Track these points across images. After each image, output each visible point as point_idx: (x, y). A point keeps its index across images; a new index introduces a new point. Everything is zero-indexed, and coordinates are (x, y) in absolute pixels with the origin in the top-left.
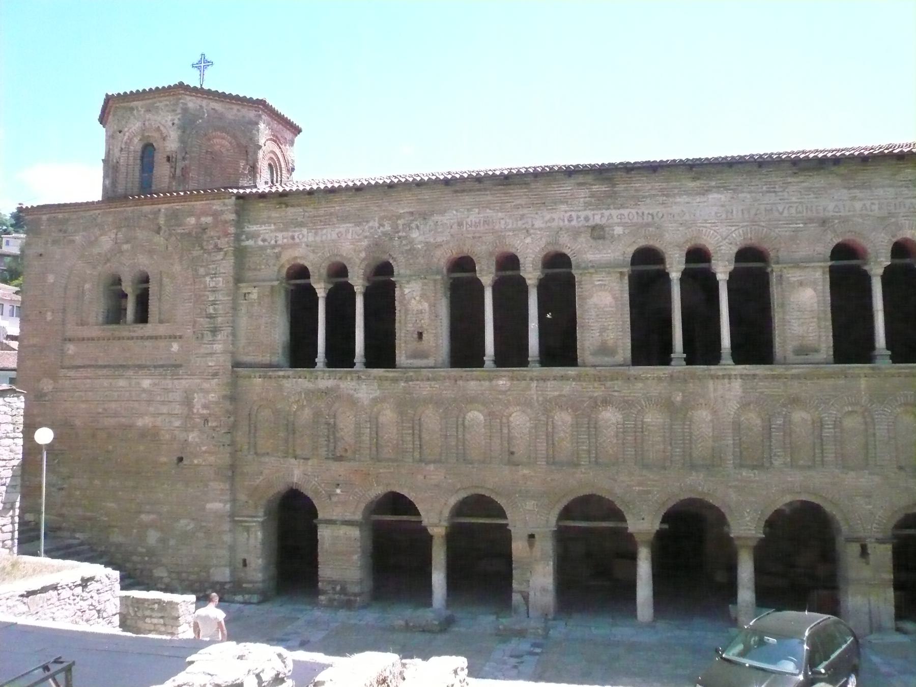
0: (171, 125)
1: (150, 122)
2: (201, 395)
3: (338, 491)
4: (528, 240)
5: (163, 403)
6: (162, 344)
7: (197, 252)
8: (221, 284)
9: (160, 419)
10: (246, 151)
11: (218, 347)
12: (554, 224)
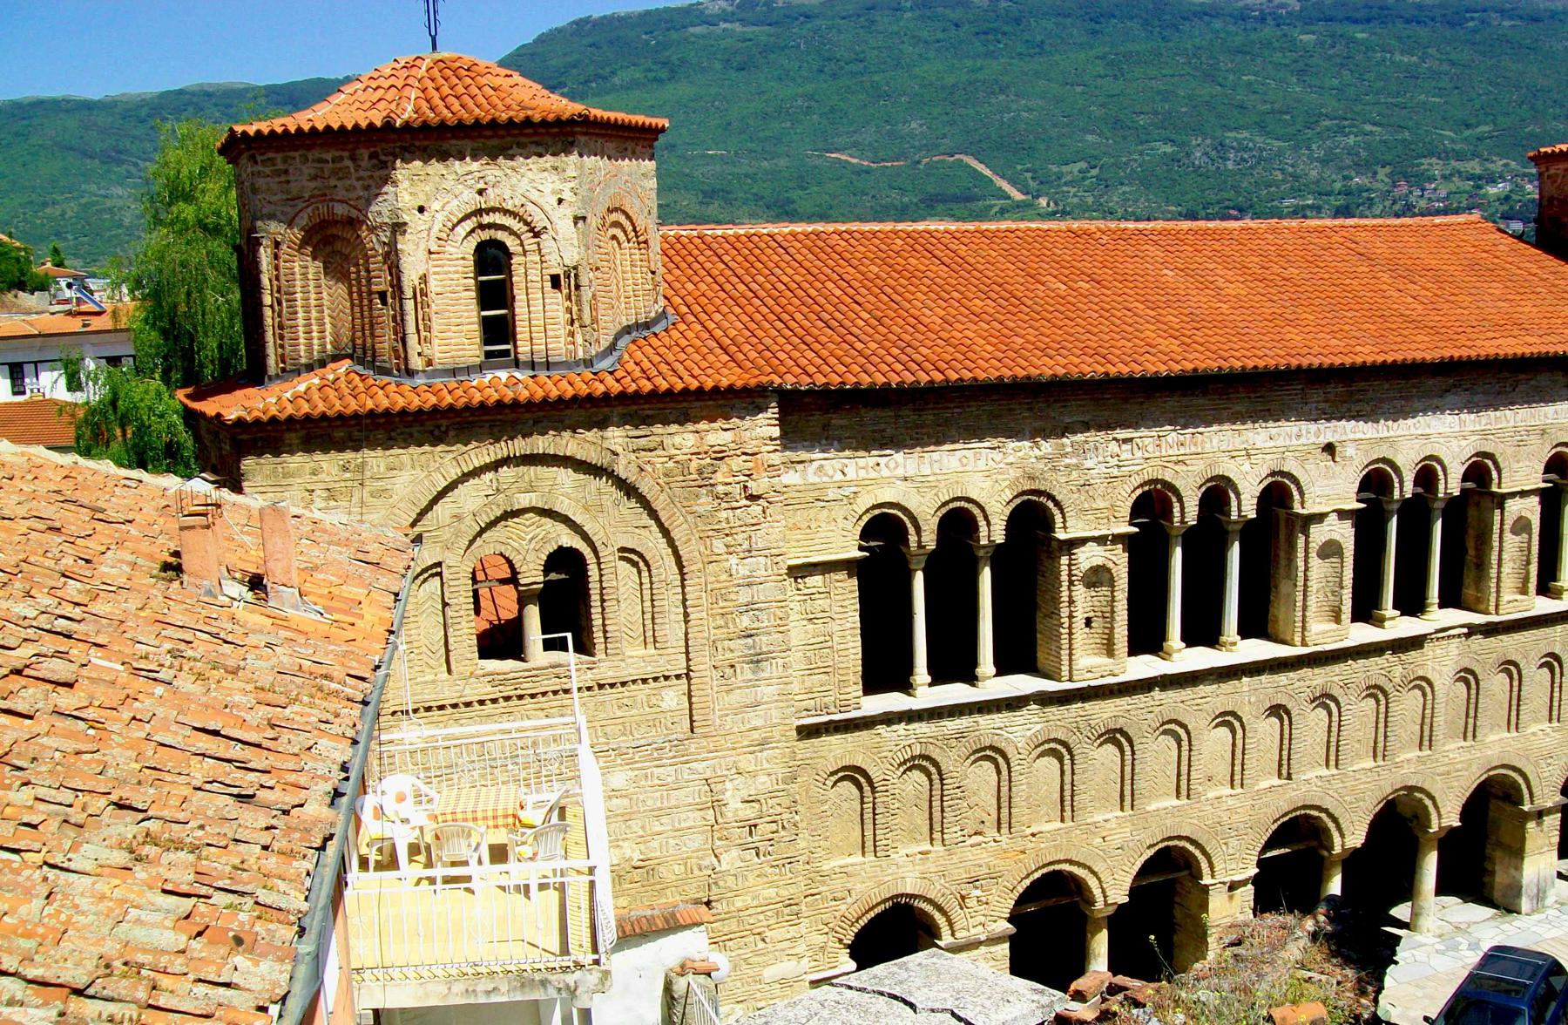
0: (556, 204)
1: (498, 191)
2: (740, 779)
3: (978, 893)
4: (1247, 467)
5: (658, 813)
6: (641, 690)
7: (705, 503)
8: (763, 572)
9: (655, 844)
10: (646, 242)
11: (767, 691)
12: (1280, 442)
